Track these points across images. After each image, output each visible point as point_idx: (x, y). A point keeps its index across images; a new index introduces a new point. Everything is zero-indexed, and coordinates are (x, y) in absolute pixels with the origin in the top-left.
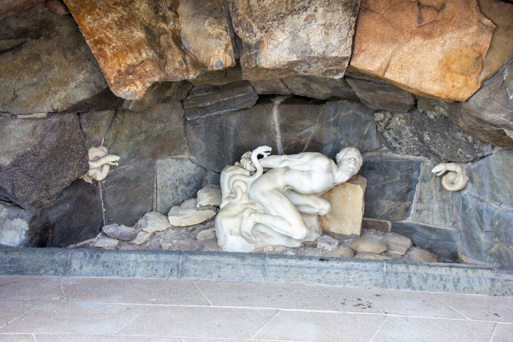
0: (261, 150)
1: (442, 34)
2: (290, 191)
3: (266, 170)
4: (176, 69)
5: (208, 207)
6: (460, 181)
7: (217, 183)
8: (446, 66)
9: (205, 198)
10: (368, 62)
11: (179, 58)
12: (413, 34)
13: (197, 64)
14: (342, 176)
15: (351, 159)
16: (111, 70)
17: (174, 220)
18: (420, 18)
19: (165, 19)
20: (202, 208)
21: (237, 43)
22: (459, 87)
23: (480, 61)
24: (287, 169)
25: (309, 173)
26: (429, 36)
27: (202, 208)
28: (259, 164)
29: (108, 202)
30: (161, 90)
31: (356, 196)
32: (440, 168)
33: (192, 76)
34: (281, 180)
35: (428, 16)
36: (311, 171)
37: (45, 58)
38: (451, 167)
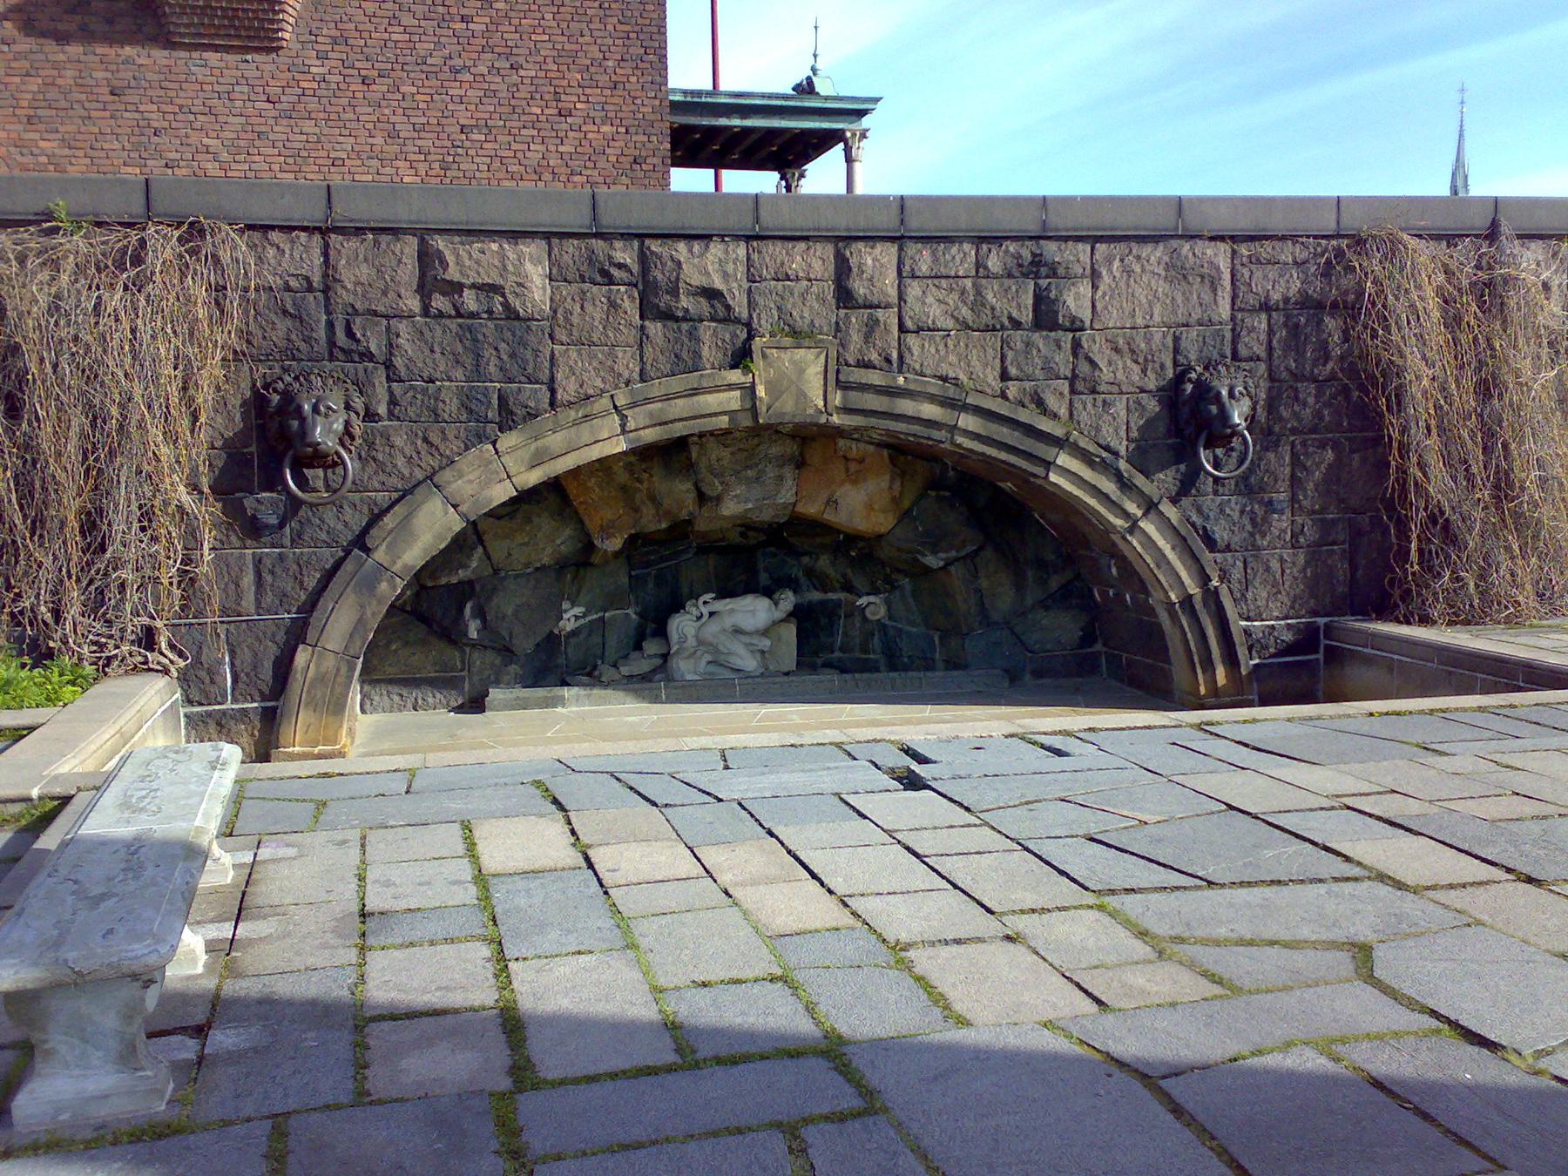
0: (707, 597)
1: (865, 480)
2: (738, 631)
3: (711, 614)
4: (652, 522)
5: (655, 655)
6: (883, 611)
7: (662, 632)
8: (870, 507)
9: (652, 647)
10: (811, 509)
11: (653, 511)
12: (842, 483)
13: (668, 513)
14: (778, 615)
15: (788, 600)
16: (592, 524)
17: (625, 670)
18: (847, 470)
19: (639, 481)
20: (650, 657)
21: (702, 497)
22: (881, 522)
23: (895, 501)
24: (732, 611)
25: (753, 612)
26: (855, 482)
27: (650, 657)
28: (705, 610)
29: (573, 652)
30: (632, 540)
31: (790, 632)
32: (863, 601)
33: (664, 526)
34: (728, 622)
35: (853, 467)
36: (754, 611)
37: (536, 520)
38: (872, 599)
